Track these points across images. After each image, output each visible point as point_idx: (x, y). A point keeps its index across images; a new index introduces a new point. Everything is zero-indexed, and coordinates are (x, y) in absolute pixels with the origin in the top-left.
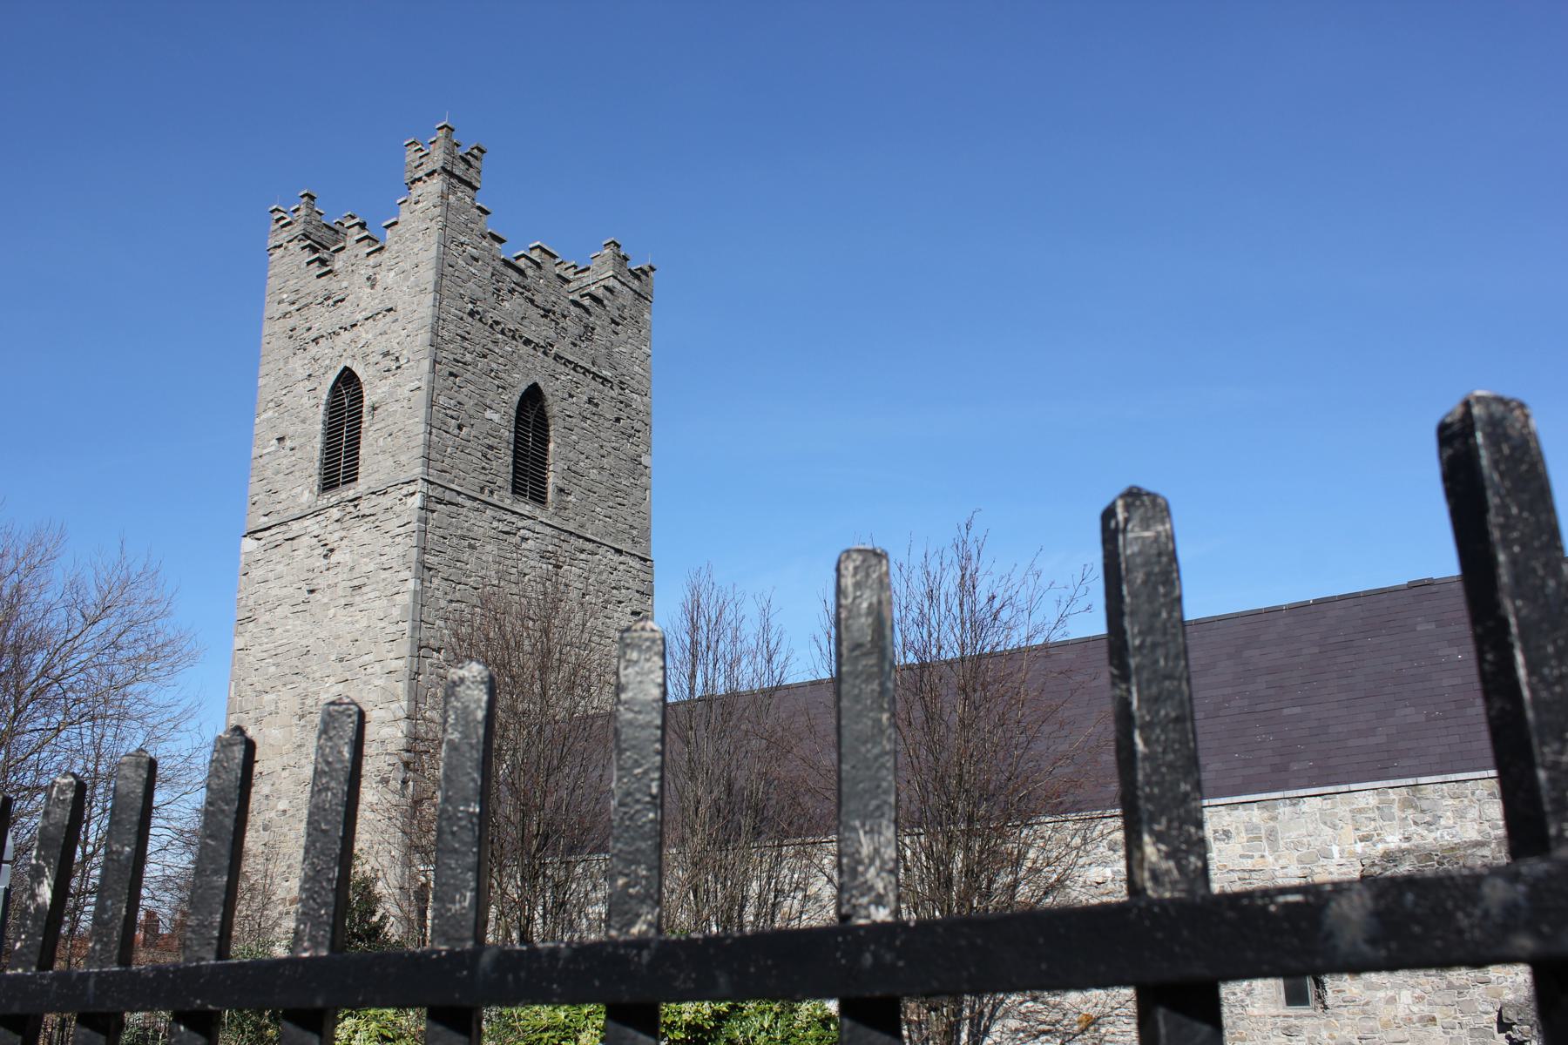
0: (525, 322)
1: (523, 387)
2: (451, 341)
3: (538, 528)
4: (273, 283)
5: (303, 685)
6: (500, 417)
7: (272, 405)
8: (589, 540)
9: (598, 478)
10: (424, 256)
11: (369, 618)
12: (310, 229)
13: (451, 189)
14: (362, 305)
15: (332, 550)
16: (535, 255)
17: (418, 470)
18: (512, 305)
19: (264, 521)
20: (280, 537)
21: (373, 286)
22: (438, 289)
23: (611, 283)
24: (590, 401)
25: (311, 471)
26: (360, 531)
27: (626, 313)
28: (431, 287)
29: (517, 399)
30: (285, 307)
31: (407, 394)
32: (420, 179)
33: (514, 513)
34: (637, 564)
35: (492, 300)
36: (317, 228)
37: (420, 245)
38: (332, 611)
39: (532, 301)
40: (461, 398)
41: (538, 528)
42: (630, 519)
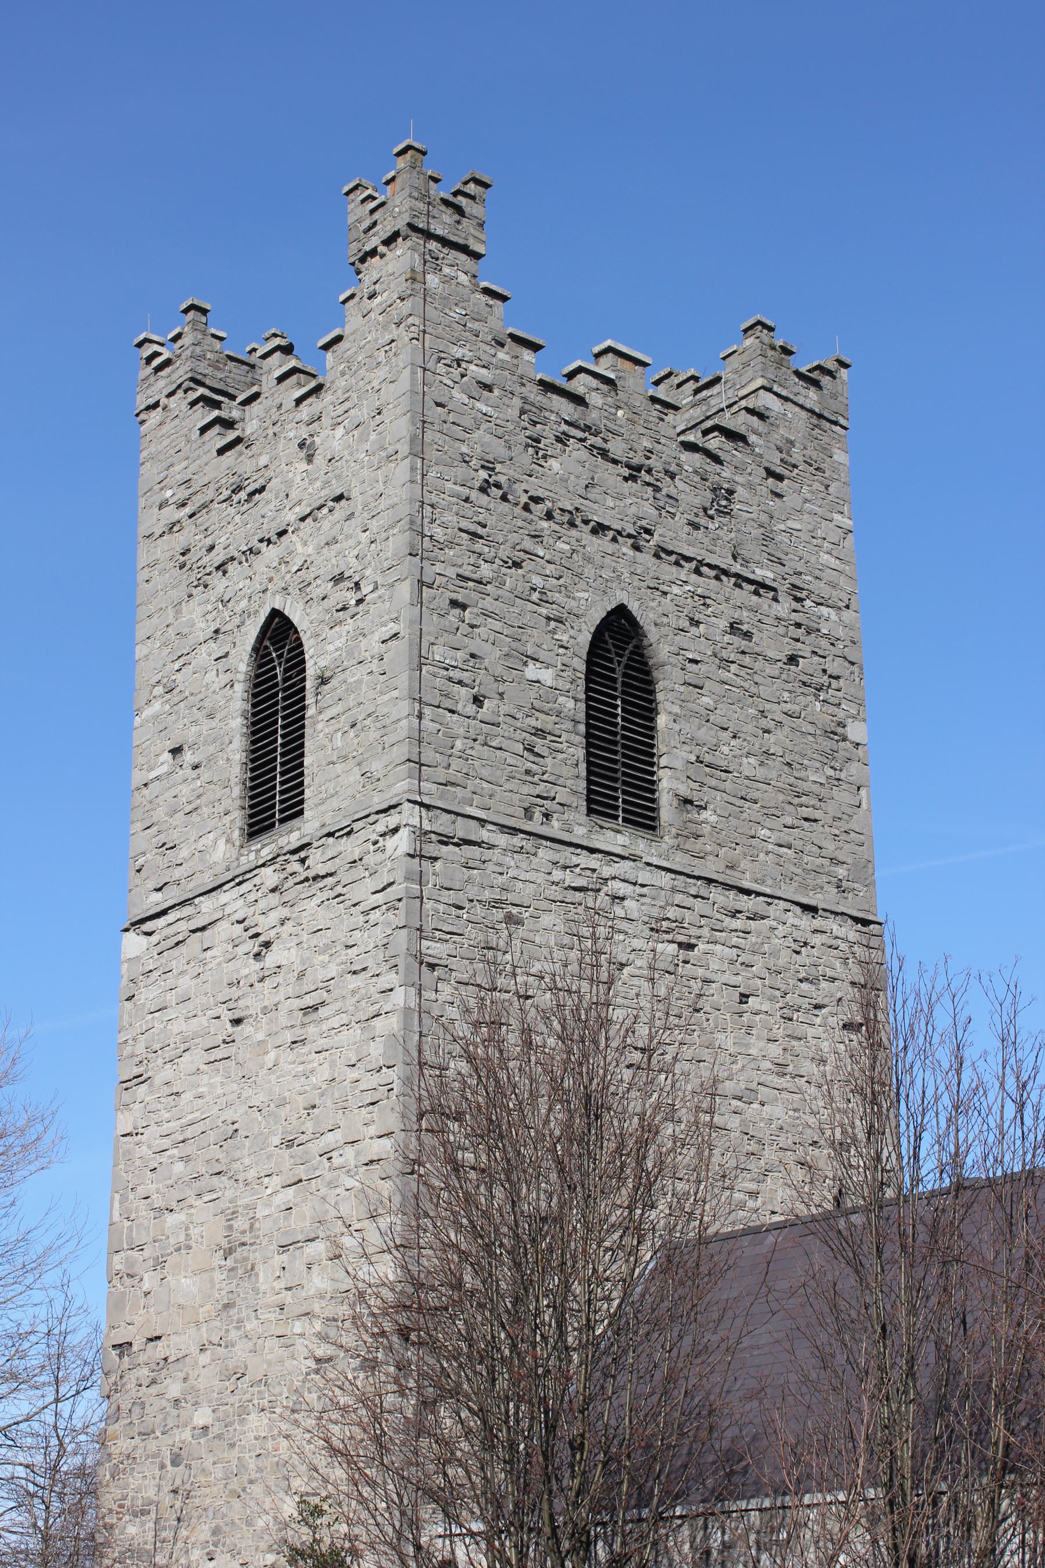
0: (593, 493)
1: (597, 615)
2: (451, 544)
3: (644, 876)
4: (150, 473)
5: (229, 1194)
6: (556, 677)
7: (159, 690)
8: (748, 892)
9: (760, 773)
10: (390, 392)
11: (333, 1065)
12: (203, 368)
13: (432, 262)
14: (294, 495)
15: (267, 945)
16: (604, 367)
17: (401, 787)
18: (566, 469)
19: (156, 901)
20: (183, 927)
21: (310, 458)
22: (418, 450)
23: (766, 400)
24: (734, 628)
25: (227, 803)
26: (312, 907)
27: (797, 455)
28: (404, 449)
29: (585, 638)
30: (172, 514)
31: (377, 648)
32: (373, 253)
33: (592, 851)
34: (850, 932)
35: (526, 458)
36: (215, 365)
37: (382, 373)
38: (272, 1055)
39: (604, 453)
40: (474, 646)
41: (644, 876)
42: (830, 846)
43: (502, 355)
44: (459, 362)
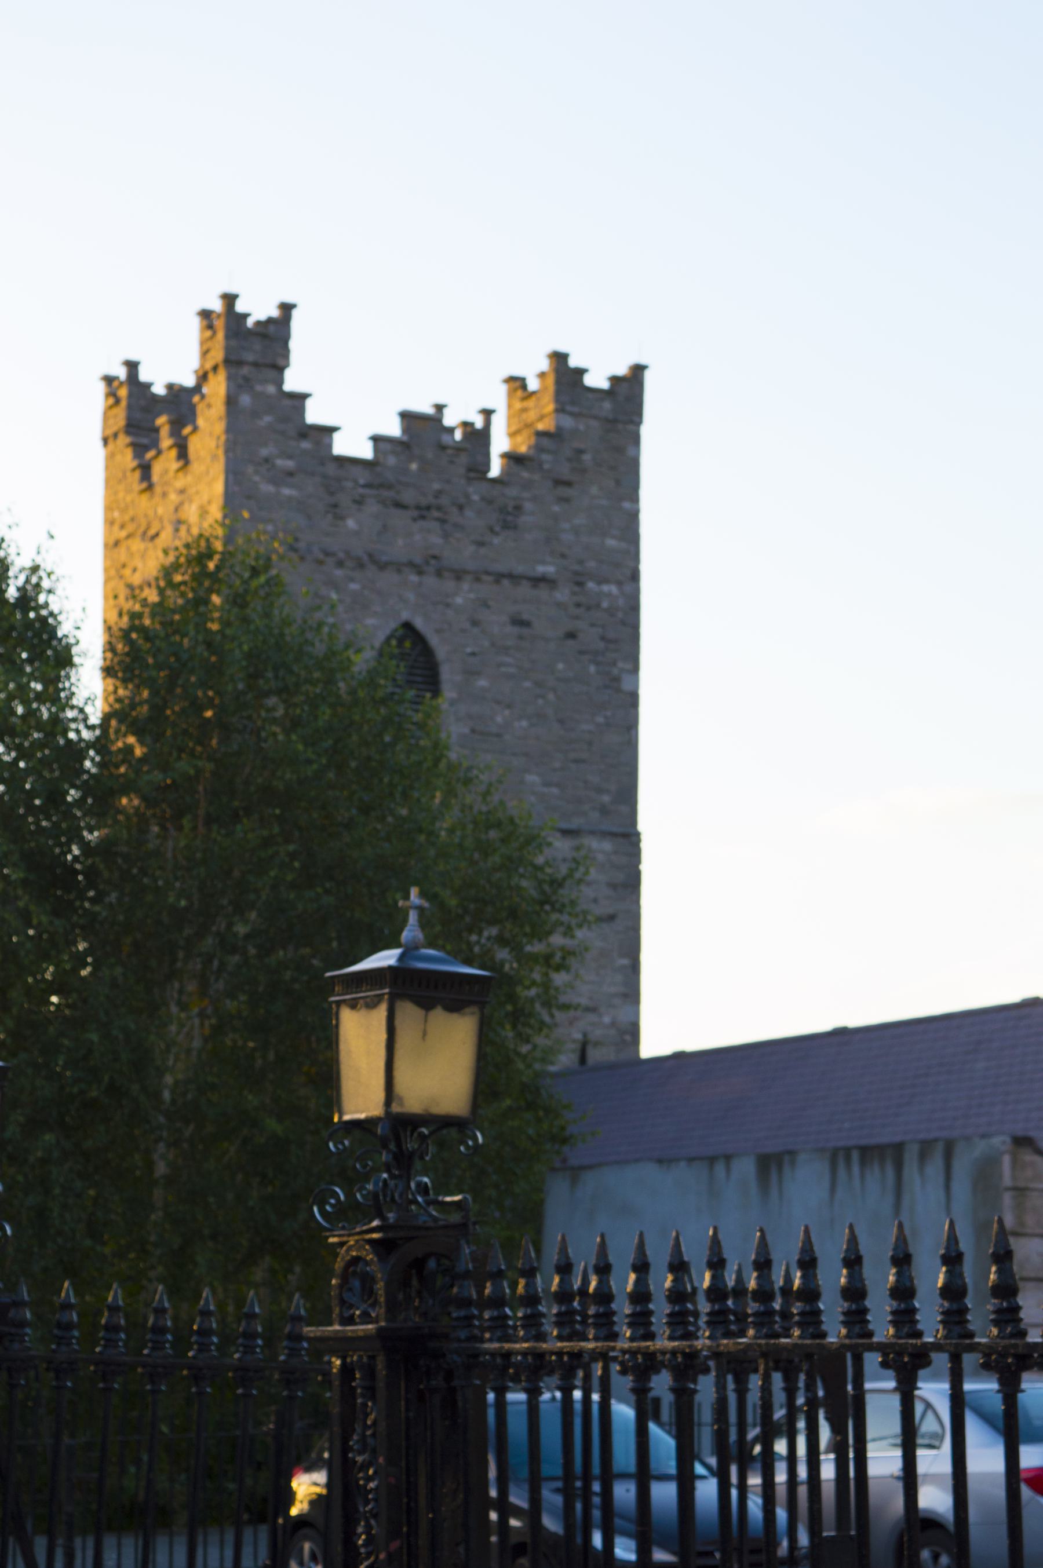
43: (305, 445)
44: (266, 460)
